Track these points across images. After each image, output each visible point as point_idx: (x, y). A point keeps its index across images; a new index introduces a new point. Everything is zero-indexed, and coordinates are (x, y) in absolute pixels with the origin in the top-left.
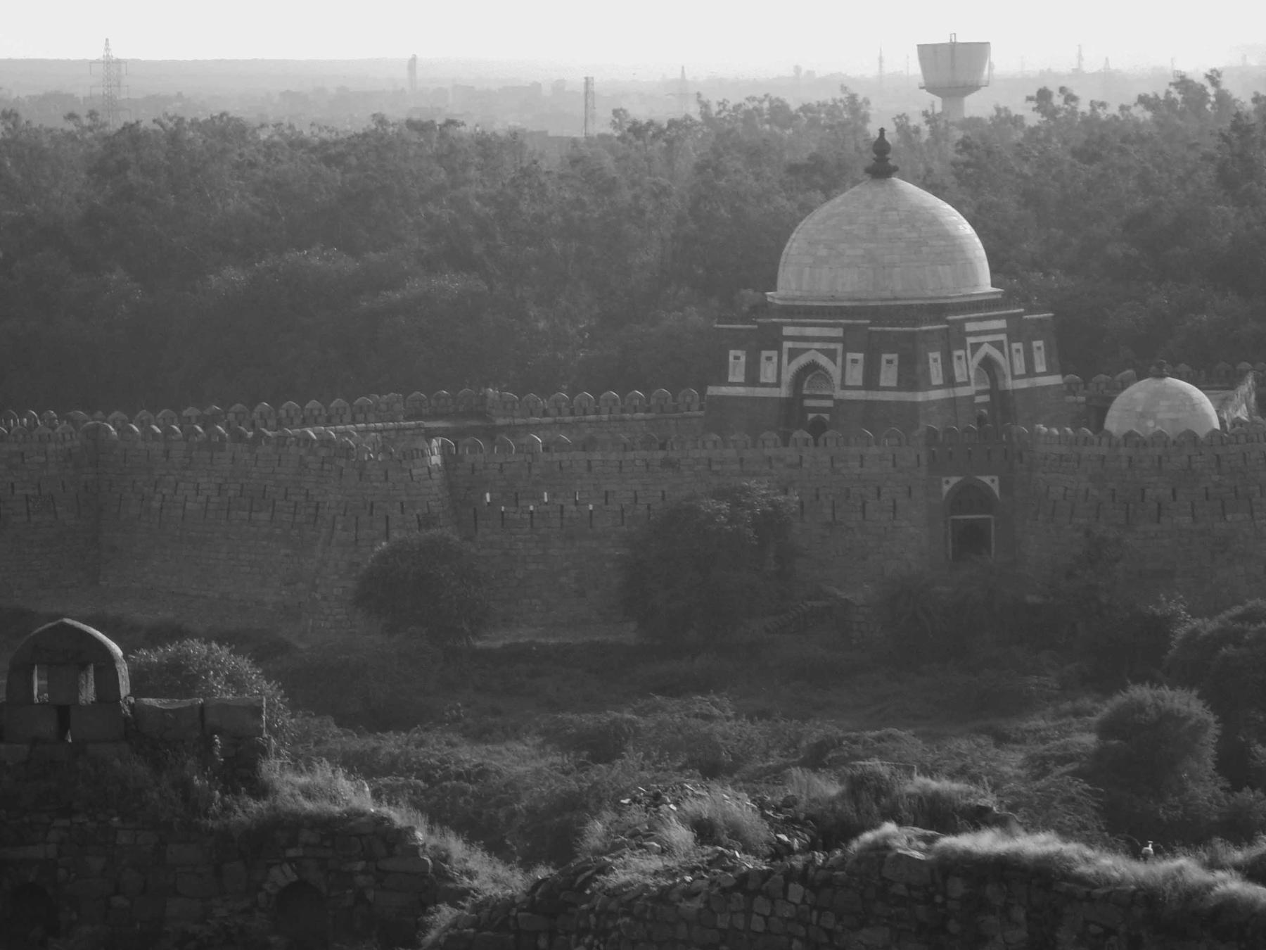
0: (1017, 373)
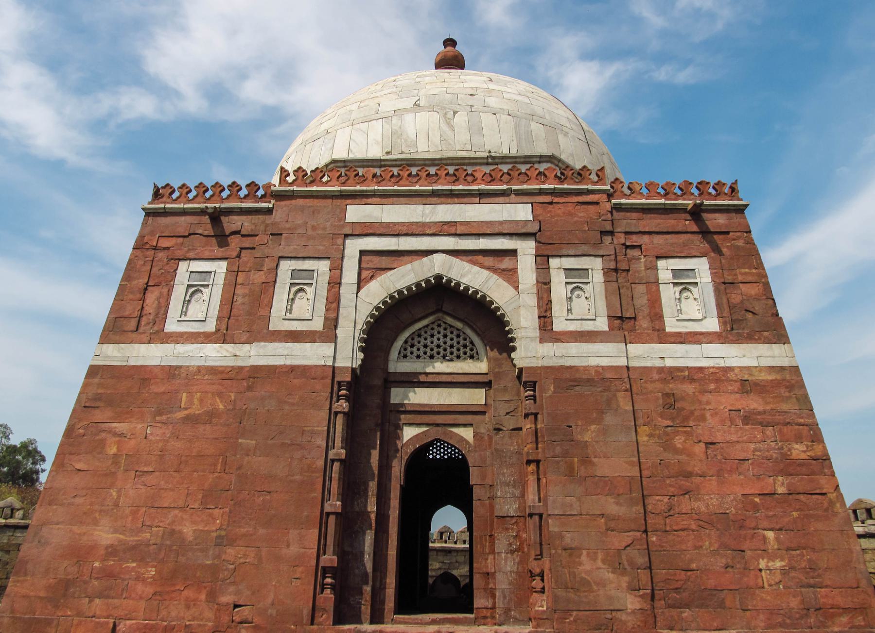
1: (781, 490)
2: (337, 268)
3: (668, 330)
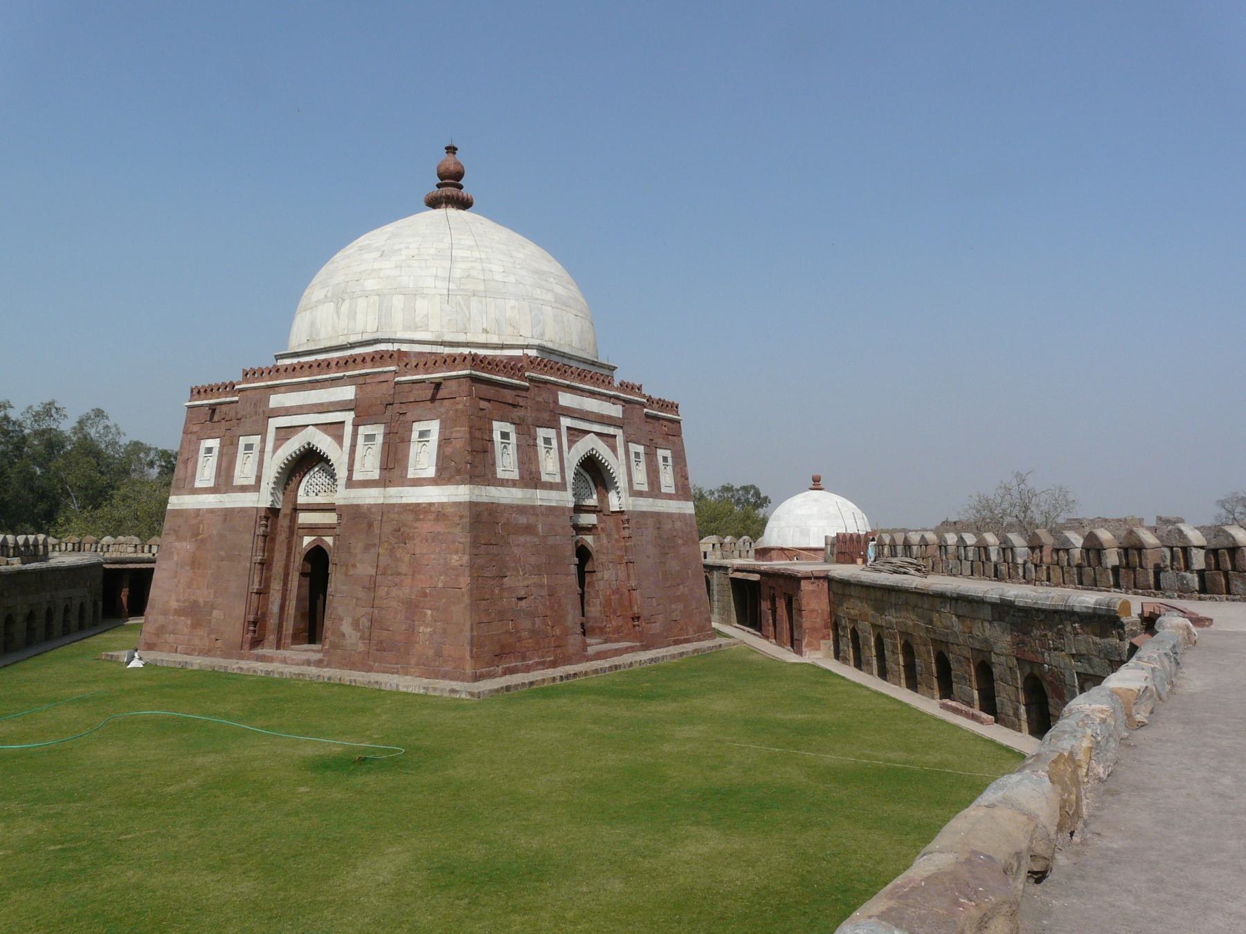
0: (637, 487)
1: (440, 585)
2: (263, 441)
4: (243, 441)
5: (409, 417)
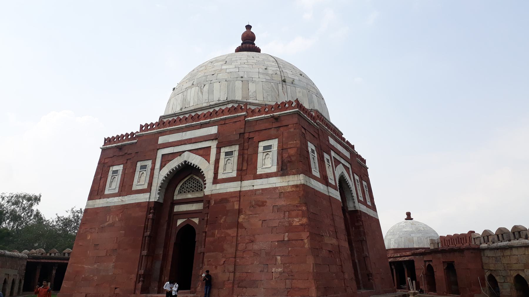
1: (286, 239)
2: (154, 164)
3: (258, 173)
4: (139, 164)
5: (256, 139)
